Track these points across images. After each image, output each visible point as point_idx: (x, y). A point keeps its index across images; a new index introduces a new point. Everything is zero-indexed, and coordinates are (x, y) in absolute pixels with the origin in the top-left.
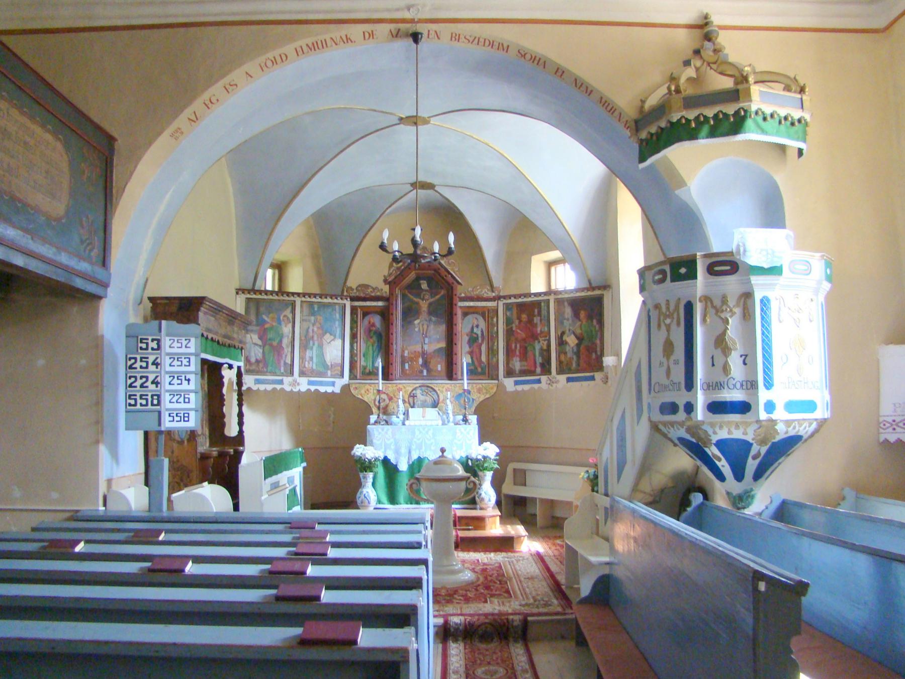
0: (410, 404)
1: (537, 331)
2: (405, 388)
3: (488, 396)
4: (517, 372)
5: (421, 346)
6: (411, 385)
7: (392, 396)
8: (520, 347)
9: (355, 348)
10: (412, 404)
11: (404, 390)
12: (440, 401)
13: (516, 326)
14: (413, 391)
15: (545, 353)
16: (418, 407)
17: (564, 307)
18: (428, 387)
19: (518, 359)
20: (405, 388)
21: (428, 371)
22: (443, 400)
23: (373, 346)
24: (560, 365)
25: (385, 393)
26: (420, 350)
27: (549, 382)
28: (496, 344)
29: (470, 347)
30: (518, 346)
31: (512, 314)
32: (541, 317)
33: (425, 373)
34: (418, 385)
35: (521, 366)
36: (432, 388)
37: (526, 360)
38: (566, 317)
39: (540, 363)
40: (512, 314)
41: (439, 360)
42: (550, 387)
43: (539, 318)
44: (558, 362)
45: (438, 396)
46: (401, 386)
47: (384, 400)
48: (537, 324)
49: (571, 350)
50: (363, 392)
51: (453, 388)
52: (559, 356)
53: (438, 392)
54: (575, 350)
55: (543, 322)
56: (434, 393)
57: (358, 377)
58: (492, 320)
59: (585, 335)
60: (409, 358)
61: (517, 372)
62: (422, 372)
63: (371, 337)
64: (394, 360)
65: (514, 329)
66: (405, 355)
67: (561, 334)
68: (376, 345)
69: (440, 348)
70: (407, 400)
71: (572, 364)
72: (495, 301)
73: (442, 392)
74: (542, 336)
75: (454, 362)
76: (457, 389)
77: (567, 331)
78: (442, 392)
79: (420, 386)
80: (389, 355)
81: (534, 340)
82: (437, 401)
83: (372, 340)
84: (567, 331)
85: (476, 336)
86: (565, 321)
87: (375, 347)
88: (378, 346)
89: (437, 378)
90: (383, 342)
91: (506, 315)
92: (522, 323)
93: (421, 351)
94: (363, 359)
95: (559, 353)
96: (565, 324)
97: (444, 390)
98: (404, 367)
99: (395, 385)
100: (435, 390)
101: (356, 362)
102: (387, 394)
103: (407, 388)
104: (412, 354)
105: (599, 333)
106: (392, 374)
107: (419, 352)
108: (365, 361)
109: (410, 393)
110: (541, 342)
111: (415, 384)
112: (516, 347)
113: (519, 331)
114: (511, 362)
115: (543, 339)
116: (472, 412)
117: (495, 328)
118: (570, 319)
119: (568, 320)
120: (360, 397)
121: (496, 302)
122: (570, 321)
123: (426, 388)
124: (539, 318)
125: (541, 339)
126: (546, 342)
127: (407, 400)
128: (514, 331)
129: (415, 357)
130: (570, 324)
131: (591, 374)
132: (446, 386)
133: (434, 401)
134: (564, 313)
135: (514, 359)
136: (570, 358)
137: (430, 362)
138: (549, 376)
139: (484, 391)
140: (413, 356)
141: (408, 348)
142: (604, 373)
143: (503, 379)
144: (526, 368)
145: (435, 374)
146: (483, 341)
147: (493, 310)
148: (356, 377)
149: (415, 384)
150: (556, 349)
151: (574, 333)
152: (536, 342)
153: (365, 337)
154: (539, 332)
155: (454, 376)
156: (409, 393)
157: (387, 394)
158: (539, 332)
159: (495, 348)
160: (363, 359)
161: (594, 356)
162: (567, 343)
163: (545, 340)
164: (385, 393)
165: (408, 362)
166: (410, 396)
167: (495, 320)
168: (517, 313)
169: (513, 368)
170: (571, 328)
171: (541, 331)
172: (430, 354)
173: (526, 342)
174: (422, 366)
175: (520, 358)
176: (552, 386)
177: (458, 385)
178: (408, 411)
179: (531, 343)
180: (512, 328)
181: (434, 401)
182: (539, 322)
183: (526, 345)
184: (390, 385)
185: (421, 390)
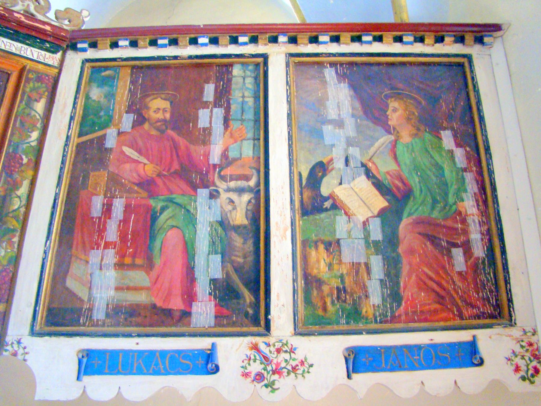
1: (207, 155)
4: (99, 315)
8: (128, 208)
13: (119, 133)
15: (238, 241)
17: (324, 83)
19: (111, 256)
24: (307, 292)
27: (256, 367)
28: (23, 191)
30: (119, 206)
31: (110, 96)
32: (228, 110)
35: (118, 289)
37: (149, 266)
38: (332, 114)
39: (214, 281)
40: (110, 96)
42: (265, 392)
43: (219, 112)
44: (301, 283)
48: (208, 132)
49: (359, 234)
52: (305, 258)
54: (377, 234)
55: (235, 125)
58: (29, 105)
59: (414, 181)
61: (99, 315)
65: (111, 142)
67: (312, 172)
71: (364, 288)
72: (53, 50)
74: (227, 172)
77: (339, 164)
81: (195, 188)
84: (339, 164)
86: (328, 129)
91: (88, 97)
92: (146, 126)
95: (305, 243)
96: (328, 140)
105: (469, 177)
110: (224, 196)
112: (108, 210)
113: (128, 151)
114: (77, 268)
115: (232, 184)
117: (35, 135)
118: (350, 124)
119: (339, 124)
121: (59, 55)
122: (350, 130)
124: (219, 112)
125: (222, 186)
126: (246, 197)
128: (109, 150)
130: (349, 143)
131: (464, 336)
134: (322, 102)
135: (95, 256)
136: (355, 267)
138: (260, 341)
142: (516, 332)
143: (29, 341)
144: (142, 298)
147: (40, 78)
150: (293, 224)
151: (369, 174)
152: (203, 193)
154: (215, 158)
158: (215, 158)
159: (16, 204)
161: (458, 254)
162: (336, 206)
163: (240, 191)
167: (40, 107)
168: (132, 93)
169: (82, 293)
170: (354, 152)
171: (225, 155)
173: (152, 194)
175: (122, 255)
176: (270, 385)
179: (179, 199)
180: (103, 138)
182: (218, 127)
183: (156, 204)
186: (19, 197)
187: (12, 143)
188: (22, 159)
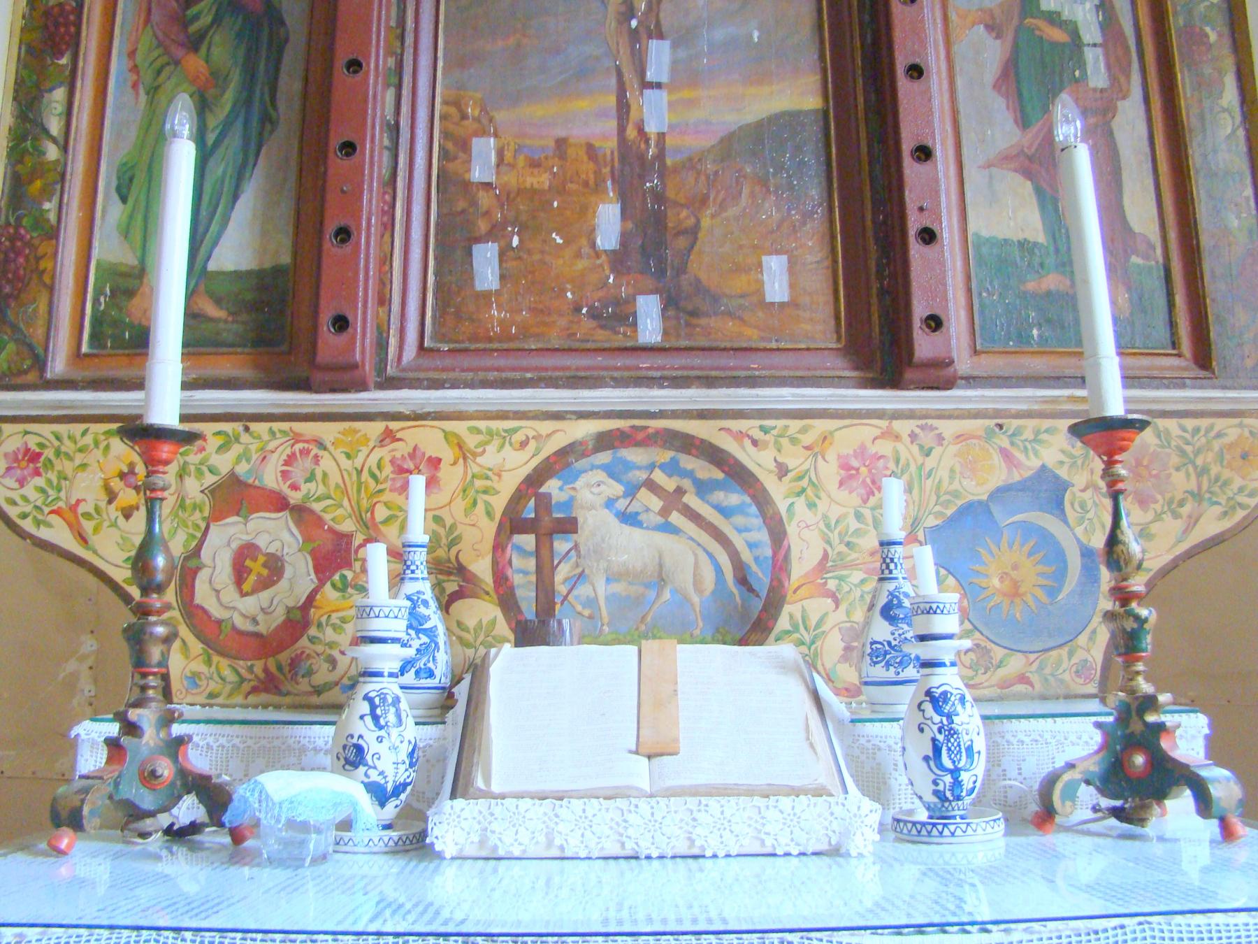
0: (507, 601)
2: (464, 453)
3: (1211, 526)
5: (612, 100)
6: (529, 428)
7: (347, 526)
9: (55, 127)
10: (529, 609)
11: (451, 476)
12: (800, 567)
14: (534, 481)
16: (592, 636)
18: (688, 444)
20: (464, 453)
21: (671, 303)
22: (823, 565)
23: (203, 107)
25: (279, 503)
26: (603, 133)
29: (1023, 122)
33: (650, 326)
34: (584, 430)
36: (716, 456)
41: (770, 211)
45: (778, 534)
46: (429, 438)
47: (275, 568)
50: (87, 489)
51: (908, 451)
53: (777, 491)
56: (734, 498)
57: (58, 365)
60: (508, 198)
62: (625, 316)
63: (195, 43)
64: (371, 201)
66: (478, 173)
68: (229, 97)
69: (775, 118)
70: (482, 568)
73: (807, 488)
75: (914, 224)
76: (945, 460)
78: (807, 488)
79: (605, 441)
80: (321, 157)
82: (761, 578)
83: (195, 63)
85: (1058, 35)
87: (213, 121)
88: (245, 102)
89: (755, 364)
90: (290, 84)
93: (610, 145)
94: (111, 213)
97: (829, 471)
98: (468, 274)
99: (378, 427)
100: (740, 476)
101: (53, 234)
102: (301, 514)
103: (490, 458)
104: (535, 164)
106: (341, 323)
107: (591, 150)
108: (126, 233)
109: (518, 498)
111: (558, 416)
116: (1082, 670)
120: (59, 534)
123: (666, 456)
127: (482, 568)
129: (560, 189)
132: (851, 437)
133: (743, 581)
137: (694, 232)
139: (1181, 482)
140: (542, 180)
141: (500, 116)
145: (751, 336)
146: (1117, 68)
148: (40, 363)
149: (558, 416)
153: (146, 41)
155: (924, 345)
156: (499, 503)
157: (301, 514)
160: (111, 213)
164: (279, 503)
165: (495, 233)
166: (512, 523)
172: (692, 163)
174: (618, 260)
177: (949, 428)
178: (476, 672)
181: (743, 581)
184: (328, 431)
185: (612, 472)
186: (1224, 110)
187: (1179, 8)
188: (1207, 36)
